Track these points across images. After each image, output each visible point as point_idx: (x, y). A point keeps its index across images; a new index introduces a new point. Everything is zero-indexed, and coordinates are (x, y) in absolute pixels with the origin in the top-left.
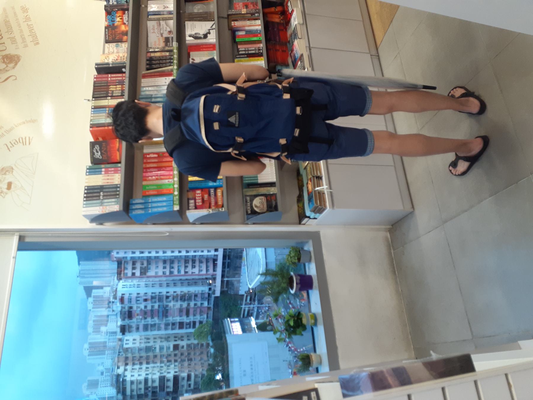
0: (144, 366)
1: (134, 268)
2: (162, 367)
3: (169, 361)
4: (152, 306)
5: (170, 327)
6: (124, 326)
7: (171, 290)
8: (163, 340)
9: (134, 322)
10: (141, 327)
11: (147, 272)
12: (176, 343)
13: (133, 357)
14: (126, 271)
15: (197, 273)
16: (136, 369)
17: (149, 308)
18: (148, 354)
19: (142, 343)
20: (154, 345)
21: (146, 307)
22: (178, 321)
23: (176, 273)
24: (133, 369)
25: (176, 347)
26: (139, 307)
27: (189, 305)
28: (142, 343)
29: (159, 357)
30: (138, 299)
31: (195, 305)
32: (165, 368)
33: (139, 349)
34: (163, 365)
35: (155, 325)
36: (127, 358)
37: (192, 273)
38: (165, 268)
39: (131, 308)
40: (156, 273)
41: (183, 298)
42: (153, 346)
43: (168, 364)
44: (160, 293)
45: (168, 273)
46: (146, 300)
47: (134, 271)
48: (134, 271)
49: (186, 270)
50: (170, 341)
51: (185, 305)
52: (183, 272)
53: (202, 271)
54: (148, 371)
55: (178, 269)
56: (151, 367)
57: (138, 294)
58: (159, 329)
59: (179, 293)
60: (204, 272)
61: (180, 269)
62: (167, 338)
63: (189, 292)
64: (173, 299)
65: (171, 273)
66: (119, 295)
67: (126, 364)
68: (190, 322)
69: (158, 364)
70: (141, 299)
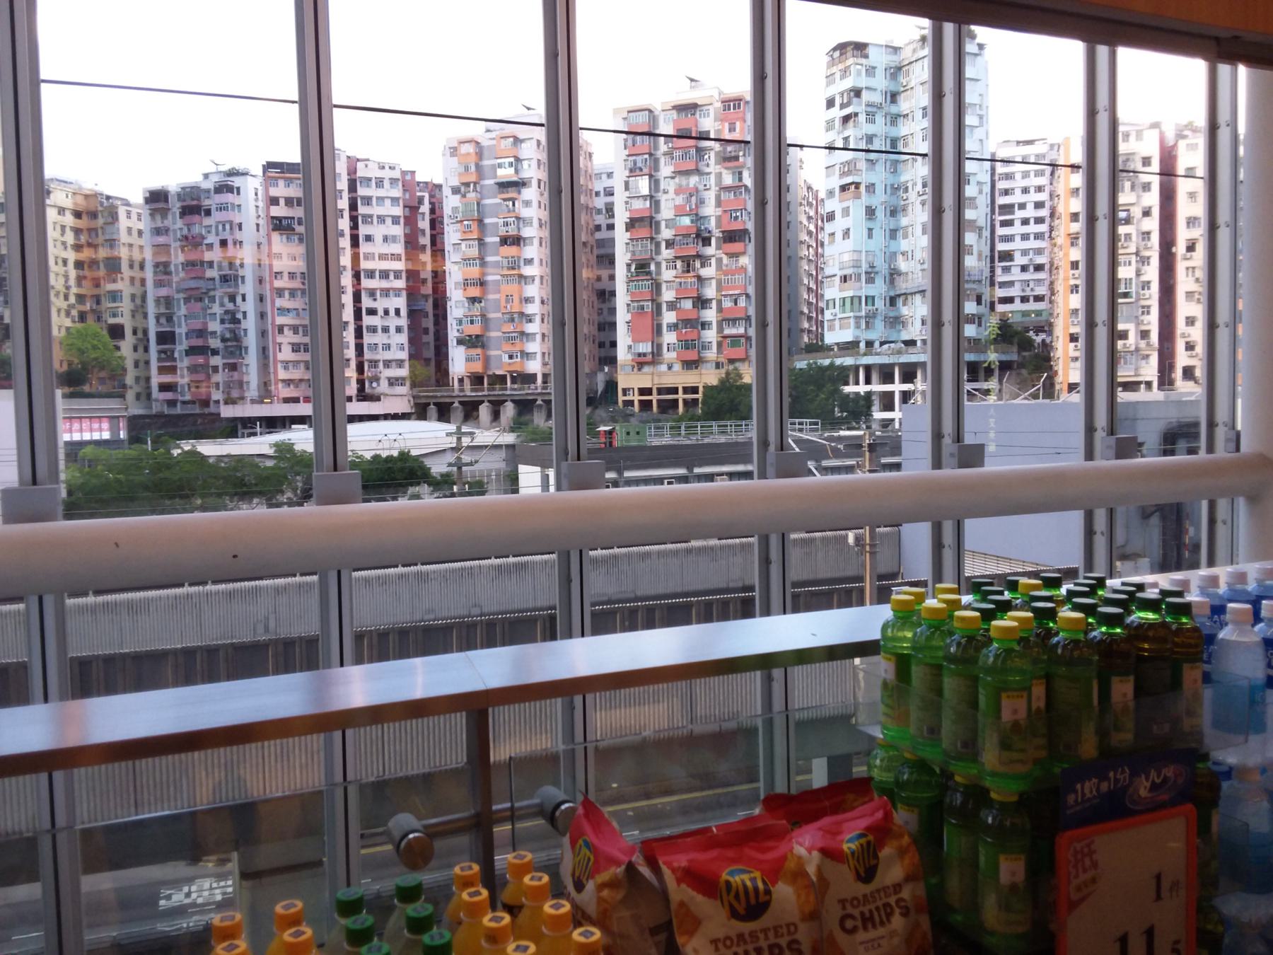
0: (71, 256)
1: (289, 202)
2: (66, 297)
3: (82, 317)
4: (211, 264)
5: (163, 310)
6: (166, 200)
7: (249, 306)
8: (138, 301)
9: (174, 223)
10: (161, 240)
11: (281, 234)
12: (128, 332)
13: (95, 230)
14: (281, 183)
15: (280, 357)
16: (62, 235)
17: (208, 256)
18: (102, 265)
19: (131, 251)
20: (122, 279)
21: (210, 246)
22: (177, 331)
23: (279, 303)
24: (63, 228)
25: (116, 332)
26: (209, 232)
27: (215, 352)
28: (131, 251)
29: (96, 292)
30: (228, 227)
31: (215, 369)
32: (64, 305)
33: (114, 240)
34: (72, 300)
35: (168, 273)
36: (93, 215)
37: (280, 344)
38: (292, 275)
39: (208, 213)
40: (279, 256)
41: (234, 344)
42: (119, 275)
43: (74, 313)
44: (243, 277)
45: (278, 284)
46: (224, 243)
47: (282, 202)
48: (282, 202)
49: (286, 329)
50: (133, 316)
51: (215, 343)
52: (280, 320)
53: (286, 368)
54: (56, 263)
55: (288, 310)
56: (66, 272)
57: (240, 226)
58: (159, 284)
59: (243, 326)
60: (282, 374)
61: (291, 315)
62: (139, 309)
63: (246, 348)
64: (227, 312)
65: (280, 293)
66: (237, 182)
67: (77, 215)
68: (175, 360)
69: (74, 290)
70: (226, 235)
